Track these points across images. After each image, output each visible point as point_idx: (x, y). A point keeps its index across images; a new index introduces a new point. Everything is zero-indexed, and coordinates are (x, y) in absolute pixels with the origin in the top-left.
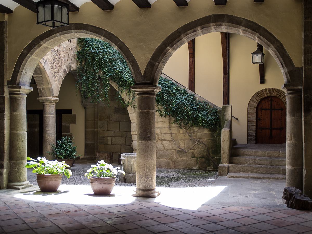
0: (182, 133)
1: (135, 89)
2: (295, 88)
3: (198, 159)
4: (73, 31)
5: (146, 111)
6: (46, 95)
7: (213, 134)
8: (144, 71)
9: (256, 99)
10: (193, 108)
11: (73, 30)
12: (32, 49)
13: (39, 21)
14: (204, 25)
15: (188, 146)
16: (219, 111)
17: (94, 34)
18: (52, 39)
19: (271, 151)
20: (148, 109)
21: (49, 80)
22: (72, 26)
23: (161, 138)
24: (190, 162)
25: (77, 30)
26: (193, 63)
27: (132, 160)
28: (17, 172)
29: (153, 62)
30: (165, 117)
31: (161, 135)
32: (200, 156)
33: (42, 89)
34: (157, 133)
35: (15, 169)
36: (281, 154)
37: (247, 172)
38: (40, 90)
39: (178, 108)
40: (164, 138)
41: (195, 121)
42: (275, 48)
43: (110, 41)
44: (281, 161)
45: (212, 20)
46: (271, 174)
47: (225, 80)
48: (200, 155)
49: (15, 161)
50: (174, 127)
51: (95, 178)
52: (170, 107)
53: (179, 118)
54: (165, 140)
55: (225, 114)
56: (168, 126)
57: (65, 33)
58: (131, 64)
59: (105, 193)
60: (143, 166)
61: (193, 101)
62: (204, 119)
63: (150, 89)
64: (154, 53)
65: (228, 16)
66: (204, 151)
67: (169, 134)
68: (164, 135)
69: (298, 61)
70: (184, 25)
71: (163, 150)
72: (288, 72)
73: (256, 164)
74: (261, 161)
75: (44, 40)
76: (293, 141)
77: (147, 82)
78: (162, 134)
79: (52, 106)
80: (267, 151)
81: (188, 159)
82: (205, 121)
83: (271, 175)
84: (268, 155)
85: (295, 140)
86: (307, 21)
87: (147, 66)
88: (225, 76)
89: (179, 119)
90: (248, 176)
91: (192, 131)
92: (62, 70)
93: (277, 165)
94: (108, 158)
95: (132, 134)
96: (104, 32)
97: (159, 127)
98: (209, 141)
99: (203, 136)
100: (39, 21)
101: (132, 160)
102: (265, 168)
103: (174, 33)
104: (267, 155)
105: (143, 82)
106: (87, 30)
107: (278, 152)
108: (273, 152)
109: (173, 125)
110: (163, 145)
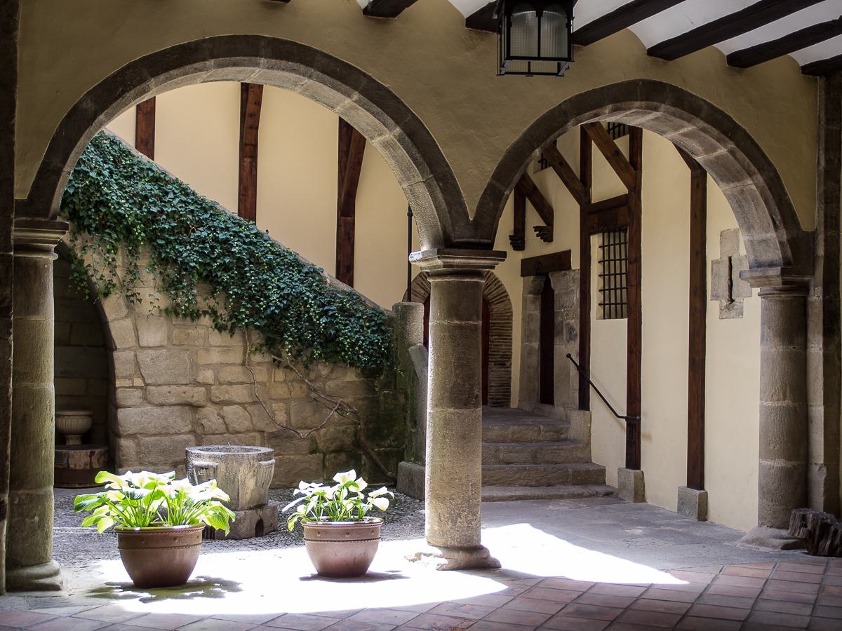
0: (281, 380)
1: (450, 258)
2: (799, 279)
3: (327, 457)
4: (263, 60)
5: (471, 322)
7: (372, 382)
8: (475, 208)
9: (422, 288)
10: (326, 308)
11: (266, 57)
12: (116, 99)
13: (512, 54)
14: (623, 103)
15: (299, 420)
16: (389, 318)
17: (332, 80)
18: (187, 74)
19: (521, 427)
20: (475, 317)
22: (262, 44)
23: (217, 397)
24: (303, 466)
25: (278, 61)
26: (254, 173)
27: (242, 469)
28: (37, 528)
29: (498, 185)
30: (232, 332)
31: (216, 389)
32: (332, 447)
34: (206, 381)
35: (33, 517)
36: (543, 433)
37: (490, 485)
39: (286, 308)
40: (227, 397)
41: (331, 348)
42: (765, 181)
43: (382, 111)
44: (557, 451)
45: (638, 93)
46: (549, 485)
47: (342, 229)
48: (332, 443)
49: (31, 489)
50: (259, 364)
51: (338, 526)
52: (261, 304)
53: (289, 336)
54: (229, 403)
55: (408, 328)
56: (239, 360)
57: (235, 65)
58: (439, 186)
59: (355, 572)
60: (464, 481)
61: (320, 289)
62: (358, 340)
63: (488, 262)
64: (502, 161)
65: (676, 90)
66: (344, 432)
67: (242, 383)
68: (228, 388)
69: (810, 216)
70: (575, 94)
72: (789, 241)
73: (499, 463)
74: (511, 454)
75: (162, 77)
76: (790, 402)
77: (482, 240)
78: (221, 384)
80: (512, 428)
81: (298, 457)
82: (360, 347)
83: (549, 487)
84: (513, 437)
85: (794, 400)
86: (830, 127)
87: (483, 196)
88: (343, 218)
89: (290, 339)
90: (509, 494)
91: (312, 376)
93: (548, 462)
96: (364, 82)
97: (211, 364)
98: (361, 402)
99: (345, 389)
100: (512, 54)
101: (242, 469)
102: (534, 472)
103: (552, 112)
104: (510, 436)
105: (473, 240)
106: (309, 64)
107: (536, 428)
108: (525, 430)
109: (257, 358)
110: (223, 418)
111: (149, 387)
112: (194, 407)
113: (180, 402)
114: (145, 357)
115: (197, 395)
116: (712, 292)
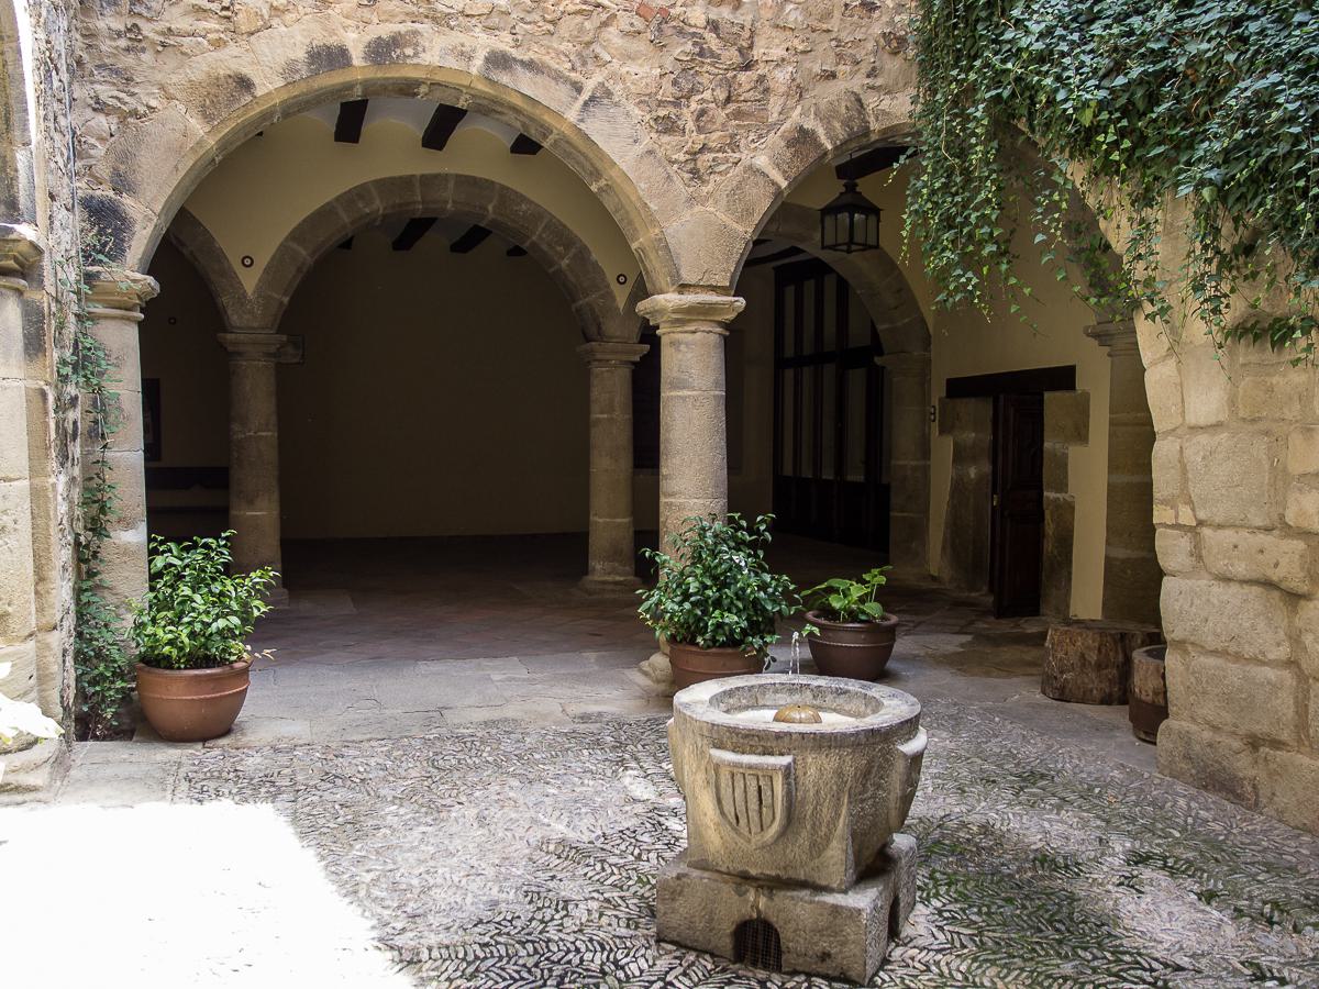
21: (640, 198)
79: (687, 344)
92: (774, 140)
94: (1099, 666)
111: (1206, 532)
113: (1254, 575)
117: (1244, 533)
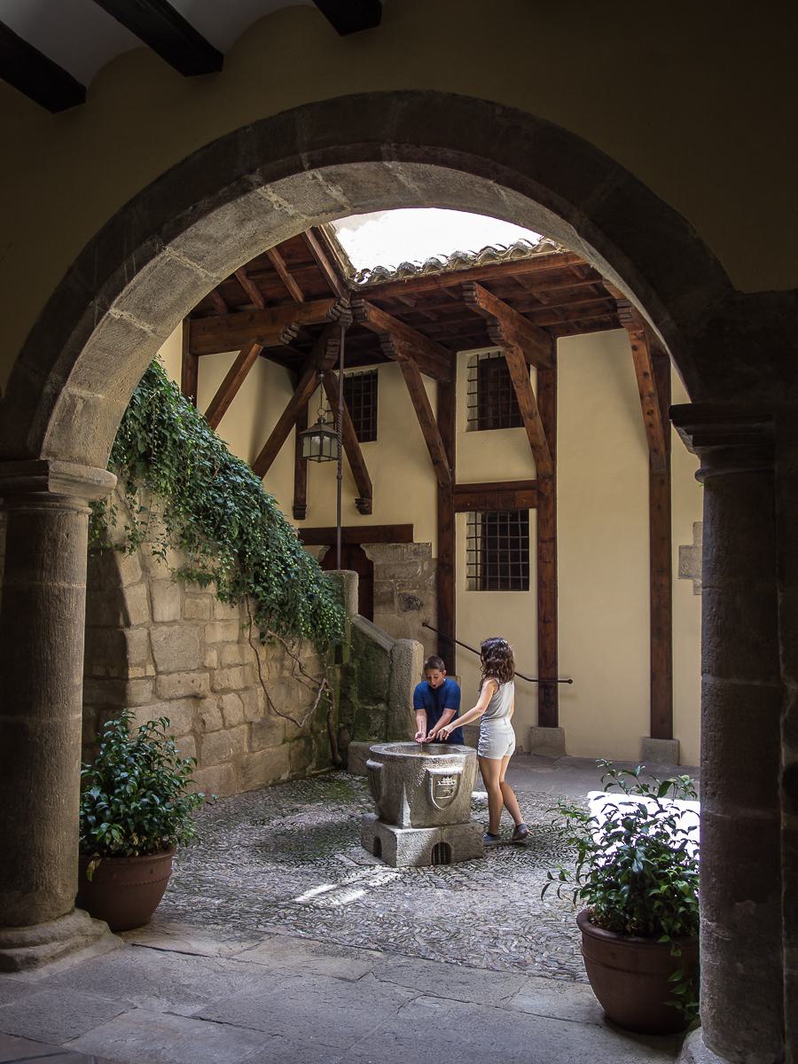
6: (83, 454)
33: (80, 406)
38: (70, 409)
56: (236, 639)
71: (218, 731)
95: (132, 673)
112: (196, 698)
113: (187, 693)
114: (159, 634)
115: (202, 682)
116: (680, 568)
117: (183, 674)
